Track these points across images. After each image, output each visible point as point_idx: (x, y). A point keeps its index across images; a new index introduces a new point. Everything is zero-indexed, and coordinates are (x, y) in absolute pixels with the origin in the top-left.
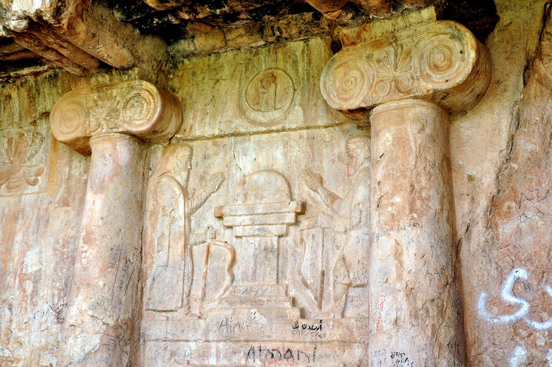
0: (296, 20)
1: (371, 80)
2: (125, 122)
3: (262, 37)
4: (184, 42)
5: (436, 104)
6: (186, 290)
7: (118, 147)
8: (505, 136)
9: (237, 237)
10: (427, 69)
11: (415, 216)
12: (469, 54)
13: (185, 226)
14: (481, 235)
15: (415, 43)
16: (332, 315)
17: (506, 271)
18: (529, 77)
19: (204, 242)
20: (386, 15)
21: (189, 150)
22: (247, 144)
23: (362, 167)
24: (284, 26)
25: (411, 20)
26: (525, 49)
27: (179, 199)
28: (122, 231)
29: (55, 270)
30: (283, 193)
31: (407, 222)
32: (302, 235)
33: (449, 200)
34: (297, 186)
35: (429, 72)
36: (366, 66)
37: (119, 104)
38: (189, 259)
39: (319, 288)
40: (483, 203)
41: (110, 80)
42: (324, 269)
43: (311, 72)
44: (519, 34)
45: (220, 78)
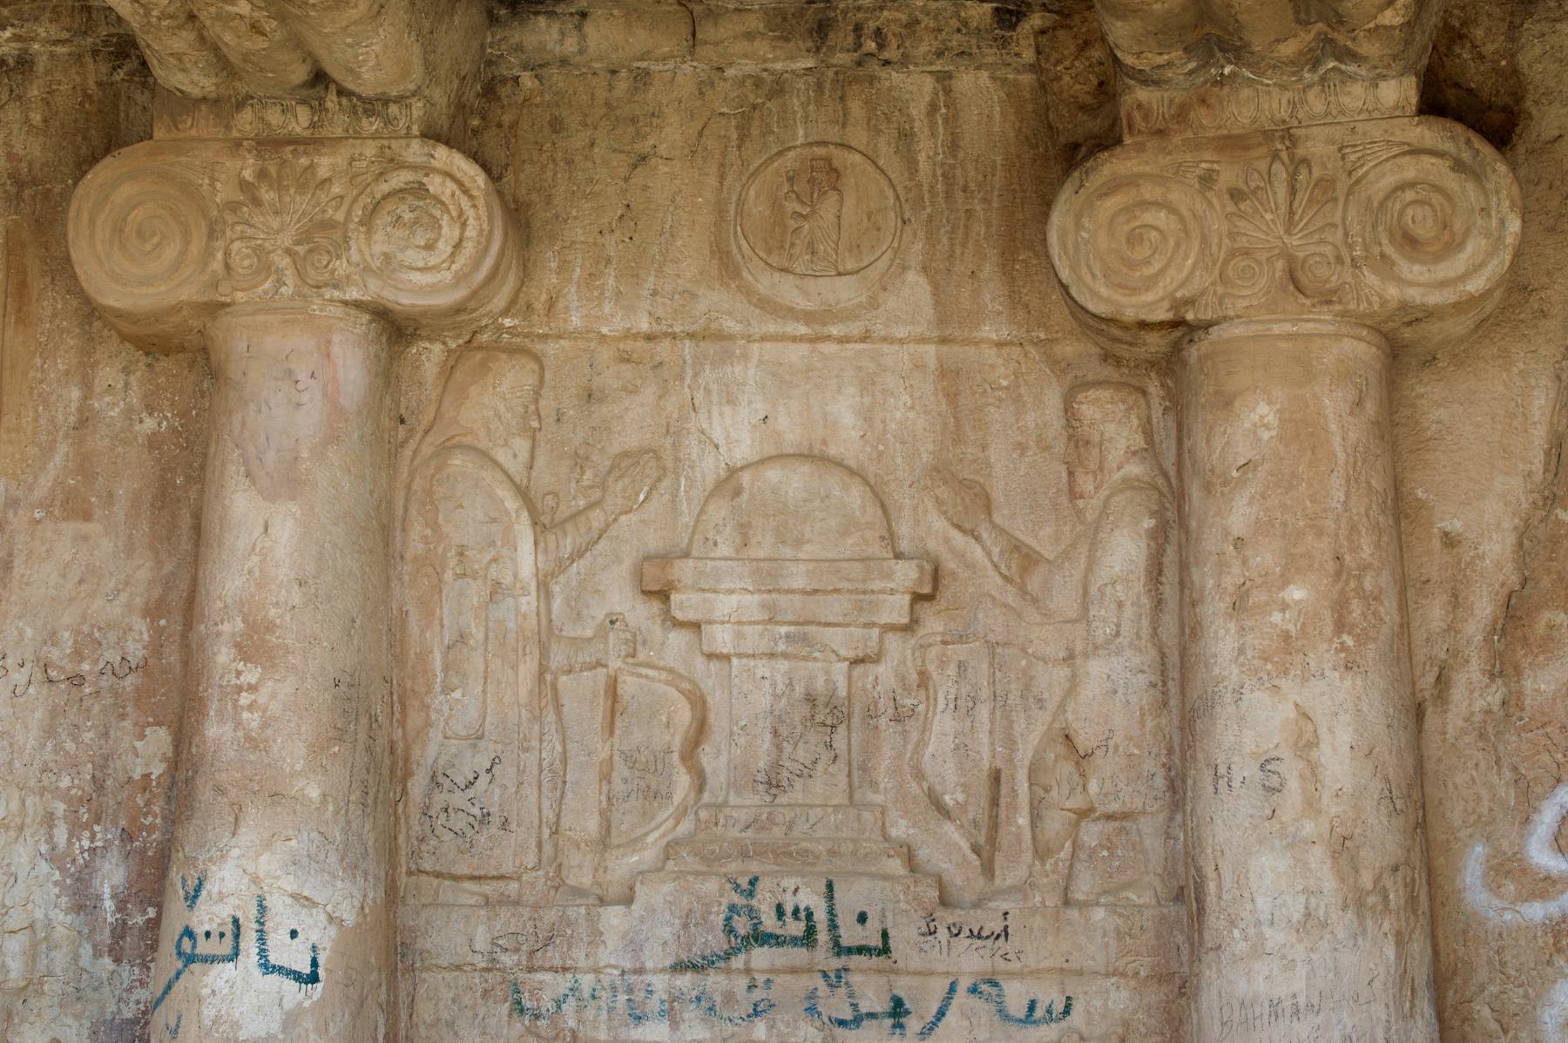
0: (936, 18)
1: (1214, 248)
2: (367, 269)
3: (818, 49)
4: (549, 26)
6: (549, 815)
7: (336, 350)
9: (711, 656)
10: (1385, 242)
11: (1349, 641)
12: (1502, 222)
14: (1476, 694)
16: (1038, 899)
17: (1538, 790)
19: (600, 664)
21: (536, 367)
22: (738, 369)
23: (1117, 476)
24: (898, 30)
25: (1345, 100)
27: (516, 527)
28: (357, 625)
29: (50, 732)
30: (869, 534)
31: (1327, 656)
34: (906, 513)
35: (1389, 250)
36: (1199, 206)
37: (345, 207)
38: (551, 717)
39: (983, 818)
40: (1484, 607)
41: (313, 125)
42: (999, 764)
43: (958, 172)
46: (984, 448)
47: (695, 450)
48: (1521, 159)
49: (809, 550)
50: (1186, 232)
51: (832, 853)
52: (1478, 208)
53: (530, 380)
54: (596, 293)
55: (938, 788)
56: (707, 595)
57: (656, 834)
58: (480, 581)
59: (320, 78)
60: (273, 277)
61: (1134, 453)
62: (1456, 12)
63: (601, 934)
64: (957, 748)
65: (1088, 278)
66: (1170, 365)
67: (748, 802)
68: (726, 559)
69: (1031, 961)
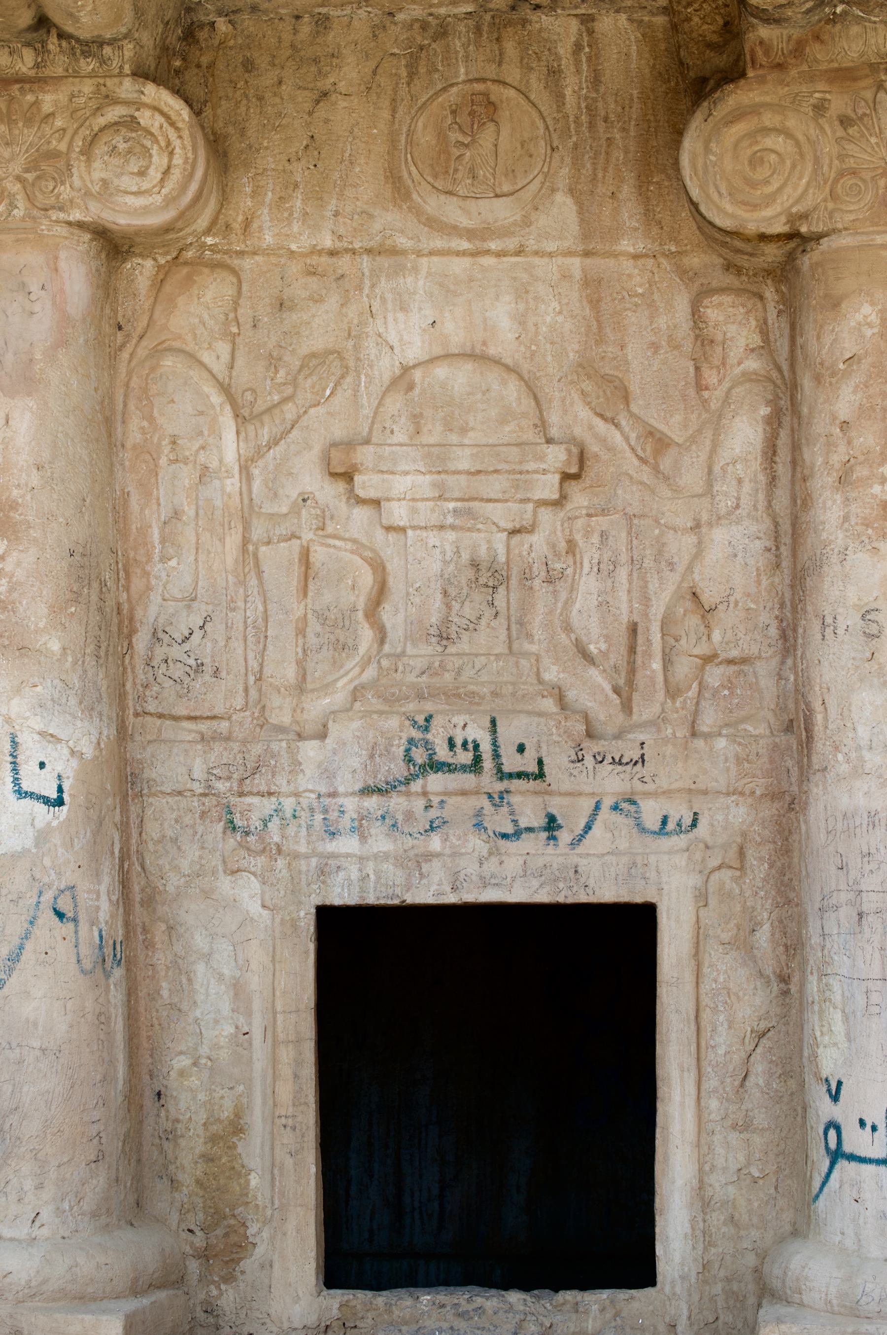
2: (88, 194)
6: (254, 664)
7: (62, 265)
9: (389, 529)
13: (241, 494)
16: (669, 731)
19: (294, 536)
21: (235, 280)
22: (409, 280)
23: (738, 370)
27: (221, 419)
32: (571, 531)
36: (813, 132)
38: (253, 582)
39: (623, 665)
41: (37, 66)
42: (636, 618)
43: (600, 104)
45: (329, 87)
46: (622, 348)
47: (373, 351)
49: (471, 438)
50: (802, 155)
51: (495, 694)
53: (230, 291)
54: (286, 215)
55: (584, 639)
56: (386, 476)
57: (345, 680)
58: (190, 466)
59: (42, 23)
60: (6, 201)
61: (753, 350)
63: (300, 764)
64: (600, 605)
65: (715, 196)
66: (785, 273)
67: (423, 652)
68: (401, 445)
69: (664, 783)
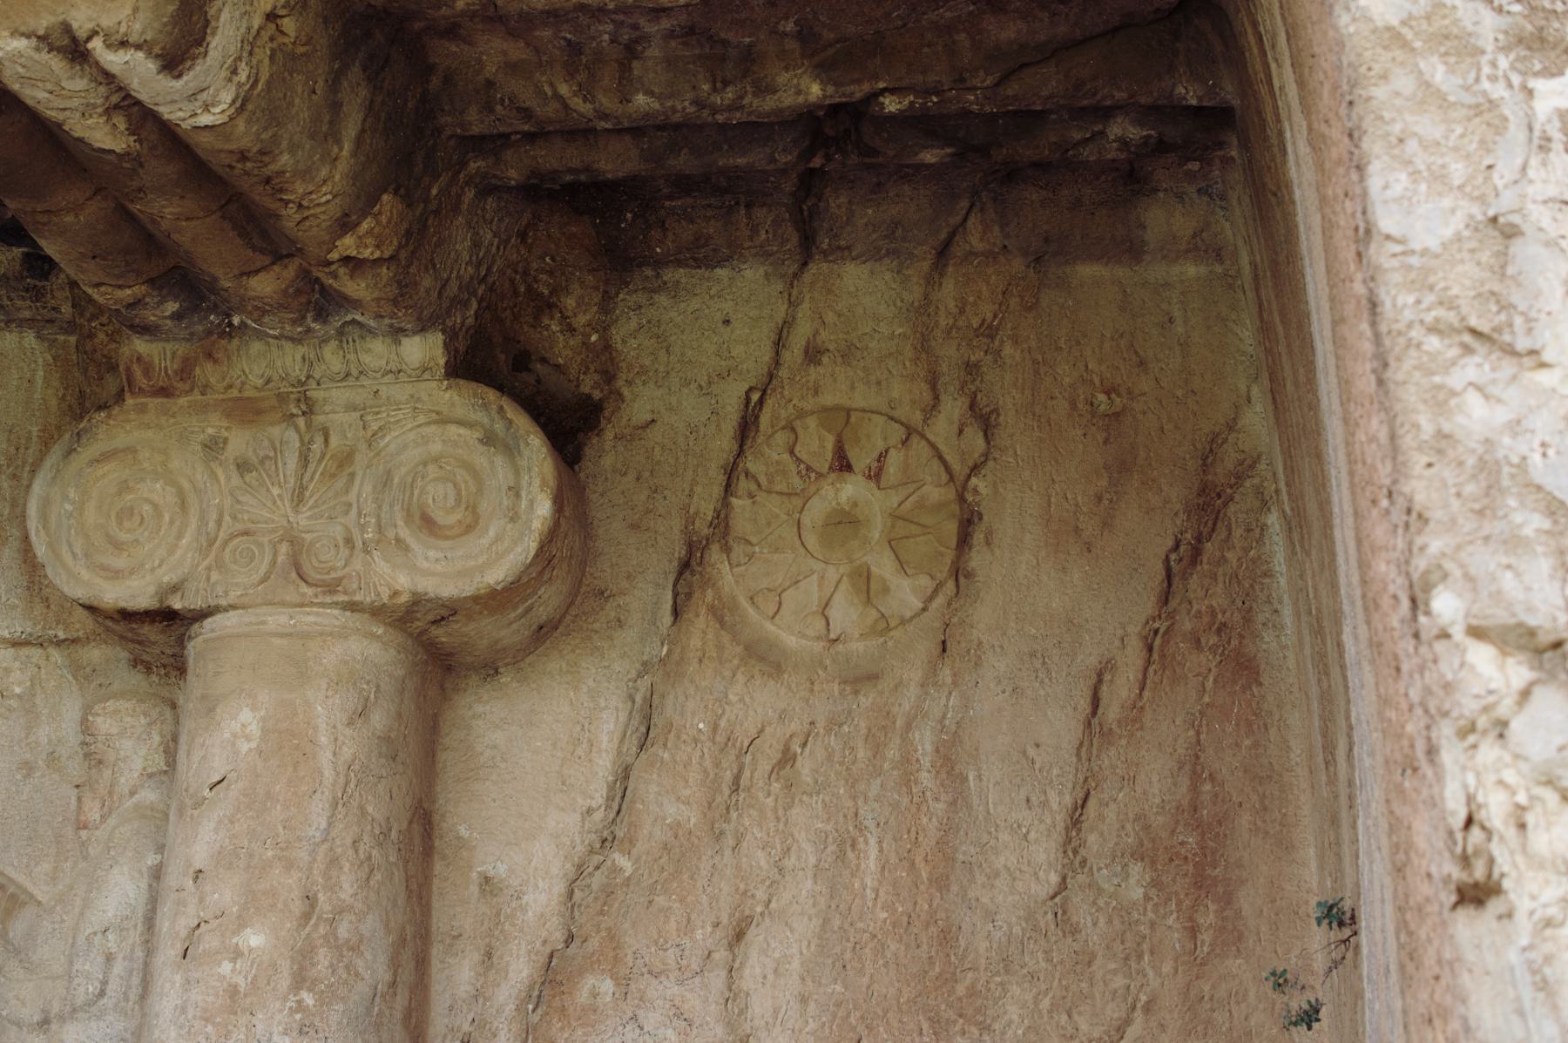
1: (212, 525)
5: (411, 635)
8: (604, 765)
10: (401, 523)
11: (309, 999)
12: (531, 503)
15: (370, 434)
18: (689, 595)
20: (288, 328)
23: (129, 804)
25: (366, 359)
26: (686, 508)
31: (278, 1017)
33: (415, 950)
35: (404, 533)
36: (201, 476)
40: (520, 969)
44: (672, 461)
48: (608, 445)
52: (505, 487)
61: (151, 776)
62: (543, 277)
